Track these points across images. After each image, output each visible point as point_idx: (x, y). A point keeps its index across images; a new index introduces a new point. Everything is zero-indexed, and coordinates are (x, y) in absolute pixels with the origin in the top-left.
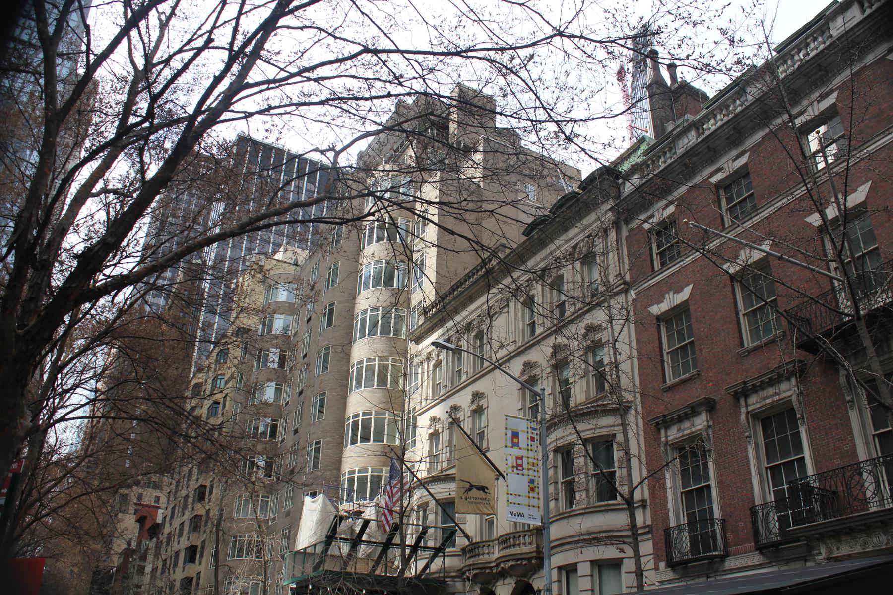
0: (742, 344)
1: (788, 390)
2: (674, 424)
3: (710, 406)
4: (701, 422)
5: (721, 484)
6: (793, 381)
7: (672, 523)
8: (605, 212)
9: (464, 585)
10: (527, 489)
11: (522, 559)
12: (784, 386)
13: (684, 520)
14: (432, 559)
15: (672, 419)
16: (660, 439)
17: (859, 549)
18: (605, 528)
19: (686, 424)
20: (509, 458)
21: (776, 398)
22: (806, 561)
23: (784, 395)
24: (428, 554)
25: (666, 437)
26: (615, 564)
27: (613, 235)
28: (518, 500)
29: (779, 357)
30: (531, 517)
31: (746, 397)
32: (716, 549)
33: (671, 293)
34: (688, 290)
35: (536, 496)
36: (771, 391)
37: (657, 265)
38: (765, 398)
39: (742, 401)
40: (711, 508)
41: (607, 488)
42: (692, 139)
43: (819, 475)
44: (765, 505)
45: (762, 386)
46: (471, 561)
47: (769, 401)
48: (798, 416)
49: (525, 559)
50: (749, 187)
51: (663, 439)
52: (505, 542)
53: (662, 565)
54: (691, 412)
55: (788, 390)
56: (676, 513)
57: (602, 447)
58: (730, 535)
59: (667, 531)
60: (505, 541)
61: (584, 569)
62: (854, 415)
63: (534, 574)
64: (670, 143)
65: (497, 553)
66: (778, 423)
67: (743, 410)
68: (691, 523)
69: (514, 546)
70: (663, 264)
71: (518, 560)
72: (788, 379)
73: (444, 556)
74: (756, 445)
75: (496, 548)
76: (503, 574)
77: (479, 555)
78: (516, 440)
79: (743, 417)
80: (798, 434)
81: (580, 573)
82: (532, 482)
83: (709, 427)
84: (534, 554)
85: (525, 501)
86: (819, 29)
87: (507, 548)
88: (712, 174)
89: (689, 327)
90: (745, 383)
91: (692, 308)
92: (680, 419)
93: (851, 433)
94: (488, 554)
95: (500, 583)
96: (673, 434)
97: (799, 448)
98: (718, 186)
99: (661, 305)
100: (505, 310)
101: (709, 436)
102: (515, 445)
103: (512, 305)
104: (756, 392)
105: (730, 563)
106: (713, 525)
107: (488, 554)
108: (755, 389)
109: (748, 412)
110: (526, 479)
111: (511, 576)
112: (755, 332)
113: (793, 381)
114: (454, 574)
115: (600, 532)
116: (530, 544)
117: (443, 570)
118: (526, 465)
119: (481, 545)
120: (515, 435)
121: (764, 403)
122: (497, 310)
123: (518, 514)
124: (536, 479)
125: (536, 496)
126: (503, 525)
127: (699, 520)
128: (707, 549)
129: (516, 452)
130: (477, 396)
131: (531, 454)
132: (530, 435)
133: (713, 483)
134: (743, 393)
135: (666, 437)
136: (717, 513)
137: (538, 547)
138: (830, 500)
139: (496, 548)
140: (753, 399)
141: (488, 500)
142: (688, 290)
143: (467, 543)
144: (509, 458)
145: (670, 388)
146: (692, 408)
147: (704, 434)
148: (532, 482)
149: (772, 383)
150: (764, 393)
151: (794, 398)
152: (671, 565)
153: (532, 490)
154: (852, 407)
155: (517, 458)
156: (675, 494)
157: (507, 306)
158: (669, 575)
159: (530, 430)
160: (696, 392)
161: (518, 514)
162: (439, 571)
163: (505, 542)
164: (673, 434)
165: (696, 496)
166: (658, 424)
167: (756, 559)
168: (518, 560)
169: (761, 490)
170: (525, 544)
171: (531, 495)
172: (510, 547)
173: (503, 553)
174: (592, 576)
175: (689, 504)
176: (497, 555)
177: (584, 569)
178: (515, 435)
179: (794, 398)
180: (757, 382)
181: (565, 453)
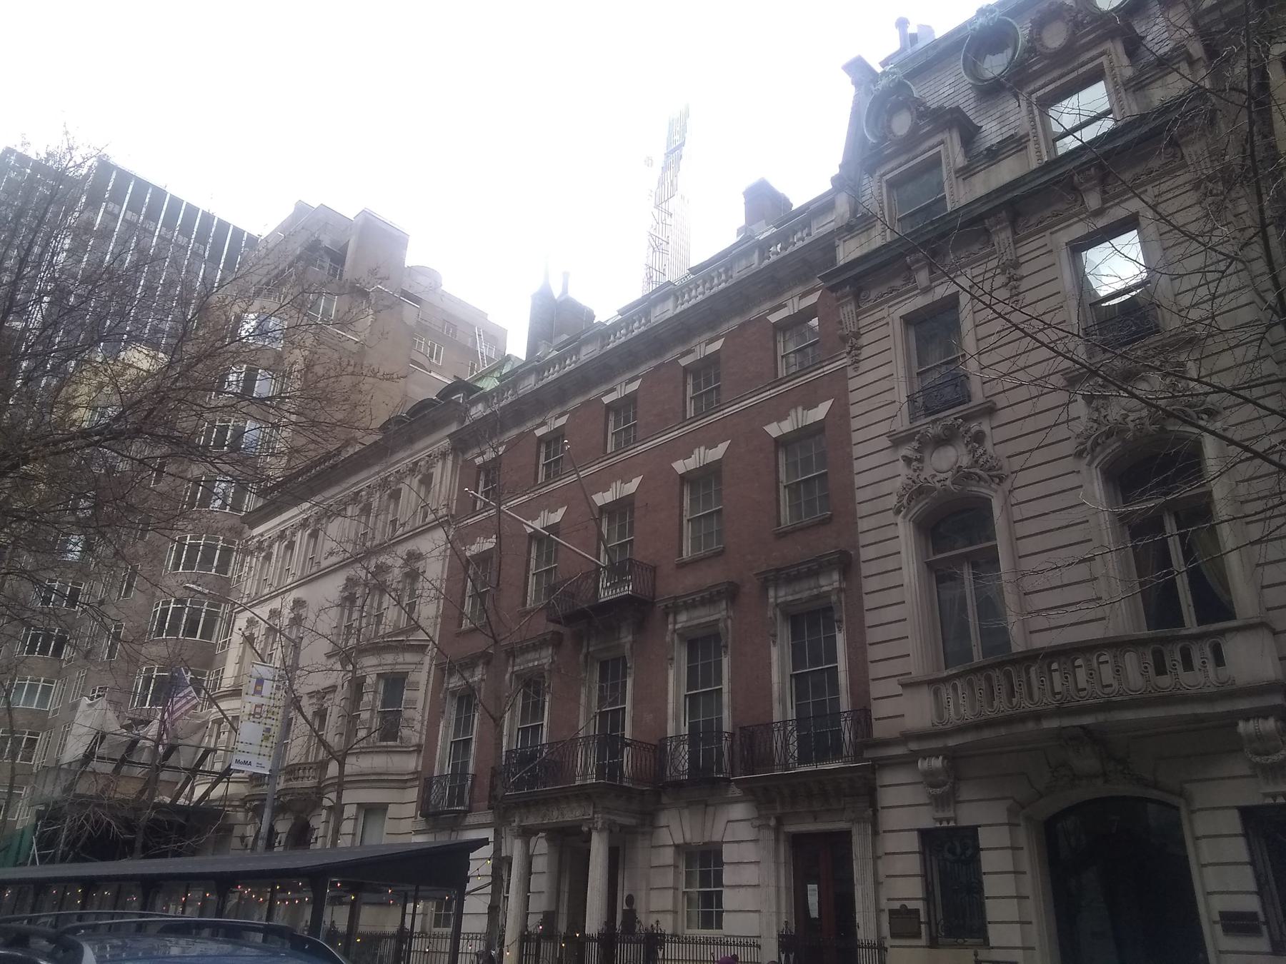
8: (440, 440)
10: (261, 737)
18: (378, 770)
24: (210, 779)
26: (381, 809)
28: (248, 748)
30: (259, 765)
41: (390, 728)
58: (476, 790)
61: (350, 811)
82: (268, 730)
85: (257, 749)
86: (574, 348)
104: (523, 654)
105: (471, 820)
110: (262, 727)
123: (245, 763)
129: (257, 700)
134: (512, 653)
136: (471, 769)
137: (320, 783)
144: (248, 706)
148: (268, 730)
153: (267, 739)
156: (444, 742)
161: (245, 763)
166: (445, 669)
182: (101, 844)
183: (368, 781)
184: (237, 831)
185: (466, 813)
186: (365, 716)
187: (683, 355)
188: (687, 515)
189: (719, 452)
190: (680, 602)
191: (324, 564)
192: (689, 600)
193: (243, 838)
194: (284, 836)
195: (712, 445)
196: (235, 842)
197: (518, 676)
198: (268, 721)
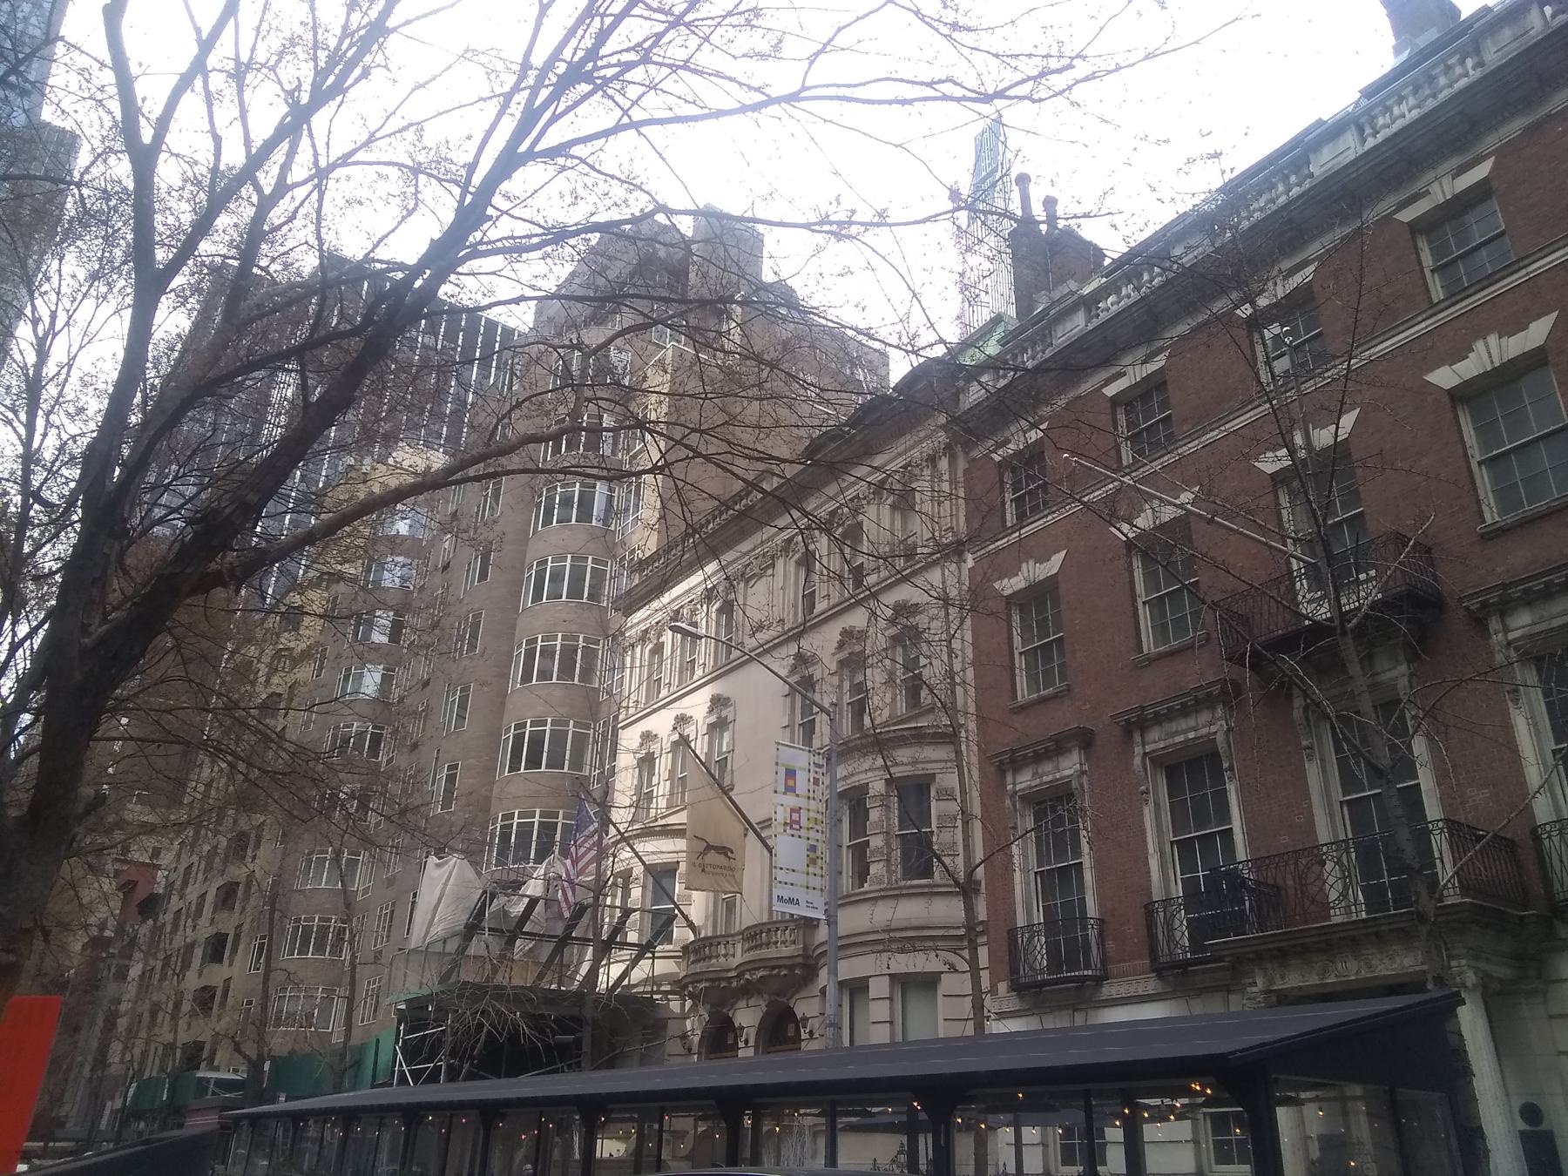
0: (1140, 649)
1: (1210, 726)
2: (1027, 765)
3: (1085, 740)
4: (1070, 765)
5: (1099, 865)
6: (1219, 712)
7: (1021, 921)
9: (683, 1006)
10: (805, 860)
11: (779, 967)
12: (1205, 717)
13: (1039, 917)
14: (634, 962)
15: (1025, 756)
16: (1005, 786)
17: (1313, 980)
18: (915, 923)
19: (1047, 767)
20: (780, 810)
21: (1191, 735)
22: (1229, 992)
23: (1204, 731)
24: (626, 954)
25: (1014, 784)
26: (927, 983)
27: (944, 464)
28: (791, 878)
29: (1201, 671)
31: (1144, 730)
32: (1087, 966)
33: (1031, 562)
34: (1058, 558)
35: (819, 872)
36: (1183, 724)
37: (1010, 519)
38: (1176, 733)
39: (1137, 738)
40: (1082, 901)
41: (919, 857)
42: (1078, 323)
43: (1256, 862)
44: (1167, 902)
45: (1170, 716)
46: (698, 968)
47: (1180, 738)
48: (1226, 765)
49: (785, 967)
50: (1165, 405)
51: (1009, 787)
52: (753, 937)
53: (1002, 987)
54: (1056, 748)
55: (1210, 726)
56: (1027, 908)
57: (913, 793)
58: (1110, 944)
59: (1012, 932)
60: (753, 935)
61: (879, 987)
62: (1312, 770)
63: (797, 992)
64: (1044, 328)
65: (739, 955)
66: (1192, 772)
67: (1138, 750)
68: (1050, 922)
69: (768, 945)
70: (1021, 517)
71: (773, 968)
72: (1212, 708)
73: (654, 958)
74: (1157, 805)
75: (739, 946)
76: (747, 991)
77: (710, 958)
78: (791, 783)
79: (1137, 761)
80: (1223, 794)
81: (872, 994)
83: (1083, 773)
84: (800, 960)
85: (800, 879)
87: (755, 947)
88: (1108, 382)
89: (1057, 616)
90: (1143, 708)
91: (1063, 588)
92: (1038, 758)
93: (1307, 796)
94: (725, 956)
95: (742, 1003)
96: (1025, 780)
97: (1225, 815)
98: (1115, 401)
99: (1014, 580)
100: (770, 572)
101: (1082, 786)
102: (790, 789)
103: (780, 563)
104: (1160, 724)
105: (1110, 990)
106: (1085, 928)
107: (725, 956)
108: (1158, 719)
109: (1145, 754)
110: (804, 844)
111: (760, 993)
112: (1161, 631)
113: (1219, 712)
114: (668, 988)
115: (906, 929)
116: (794, 942)
117: (652, 980)
118: (804, 823)
119: (715, 941)
120: (790, 774)
121: (1170, 741)
122: (756, 570)
124: (819, 845)
125: (819, 872)
126: (751, 912)
127: (1063, 918)
128: (1074, 965)
129: (790, 800)
130: (718, 702)
131: (813, 805)
132: (812, 775)
133: (1086, 861)
134: (1135, 725)
135: (1014, 784)
136: (1092, 910)
137: (805, 948)
138: (1270, 898)
139: (739, 946)
140: (1154, 734)
141: (731, 869)
142: (1058, 558)
143: (692, 938)
144: (780, 810)
145: (1023, 708)
146: (1057, 742)
147: (1075, 784)
149: (1185, 712)
150: (1173, 727)
151: (1220, 738)
152: (1018, 988)
154: (1310, 758)
155: (793, 810)
157: (773, 566)
158: (1013, 1004)
159: (812, 767)
160: (1064, 717)
162: (645, 981)
163: (753, 937)
164: (1025, 780)
165: (1059, 881)
166: (1004, 763)
167: (1151, 985)
168: (773, 968)
169: (1163, 877)
170: (784, 943)
171: (811, 870)
172: (761, 946)
173: (749, 956)
174: (890, 999)
175: (1047, 893)
176: (738, 960)
177: (879, 987)
178: (790, 774)
179: (1220, 738)
180: (1162, 709)
181: (855, 801)
182: (502, 1054)
183: (861, 944)
184: (673, 1029)
185: (1099, 981)
186: (876, 842)
187: (1402, 205)
188: (1476, 455)
189: (1537, 332)
190: (1516, 592)
191: (750, 643)
192: (1537, 585)
193: (684, 1037)
194: (752, 1033)
195: (1516, 325)
196: (674, 1047)
197: (1157, 760)
198: (812, 834)
